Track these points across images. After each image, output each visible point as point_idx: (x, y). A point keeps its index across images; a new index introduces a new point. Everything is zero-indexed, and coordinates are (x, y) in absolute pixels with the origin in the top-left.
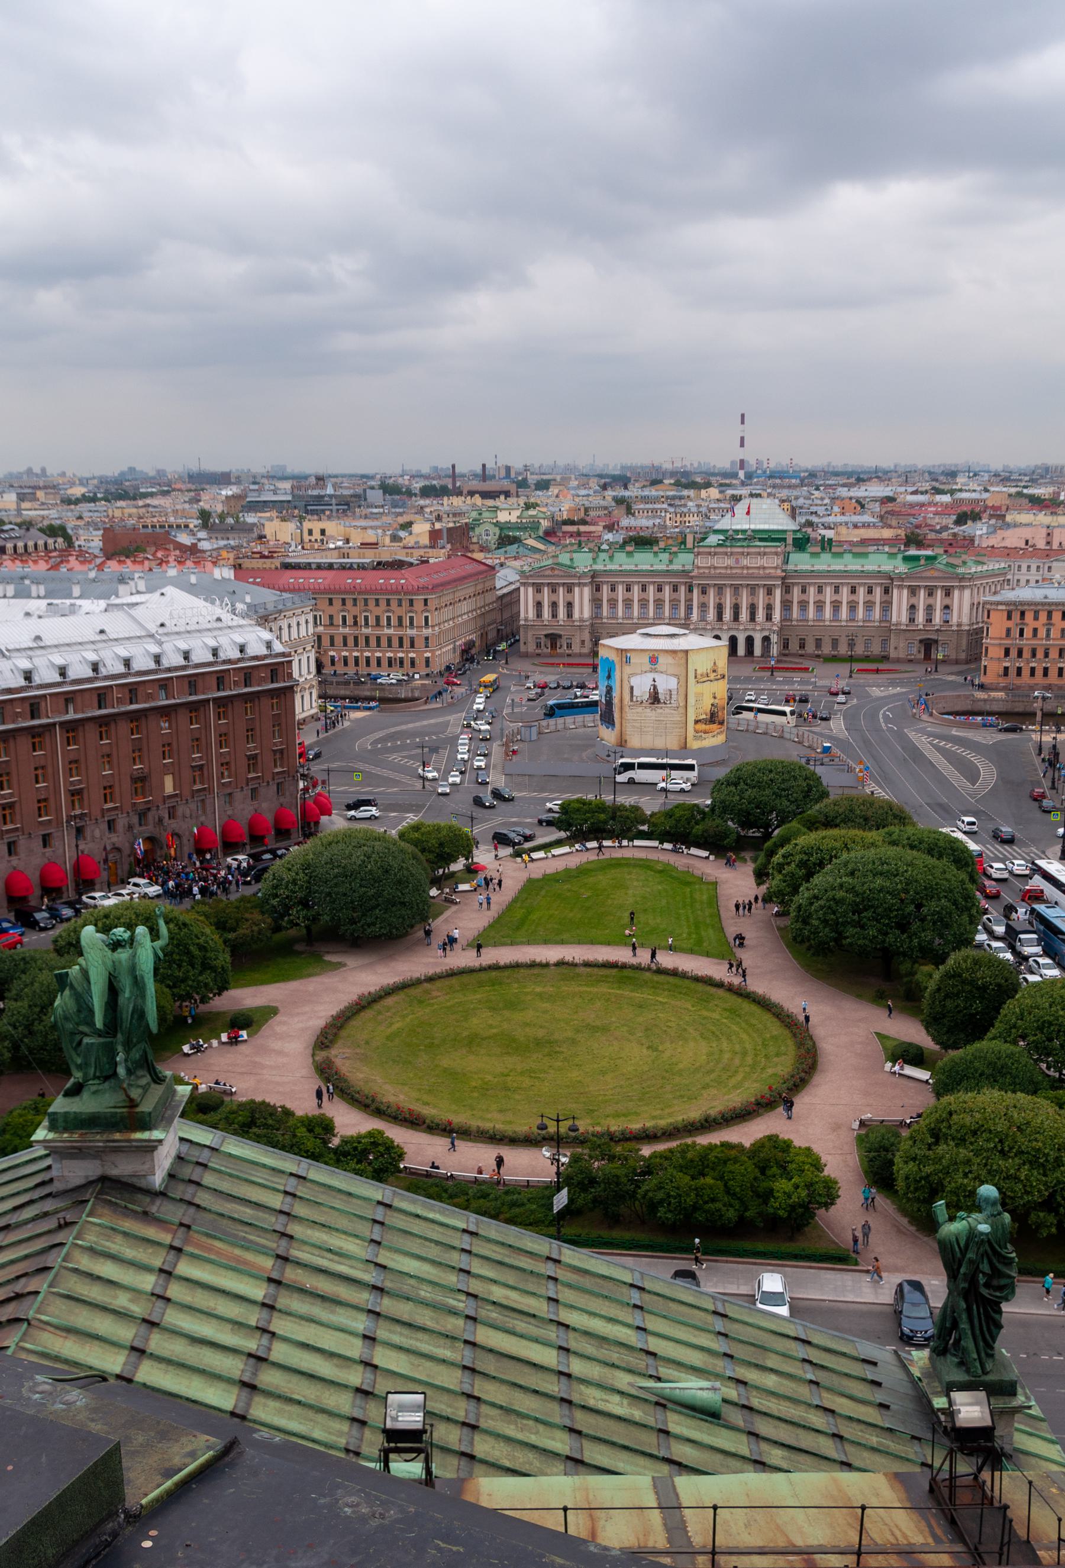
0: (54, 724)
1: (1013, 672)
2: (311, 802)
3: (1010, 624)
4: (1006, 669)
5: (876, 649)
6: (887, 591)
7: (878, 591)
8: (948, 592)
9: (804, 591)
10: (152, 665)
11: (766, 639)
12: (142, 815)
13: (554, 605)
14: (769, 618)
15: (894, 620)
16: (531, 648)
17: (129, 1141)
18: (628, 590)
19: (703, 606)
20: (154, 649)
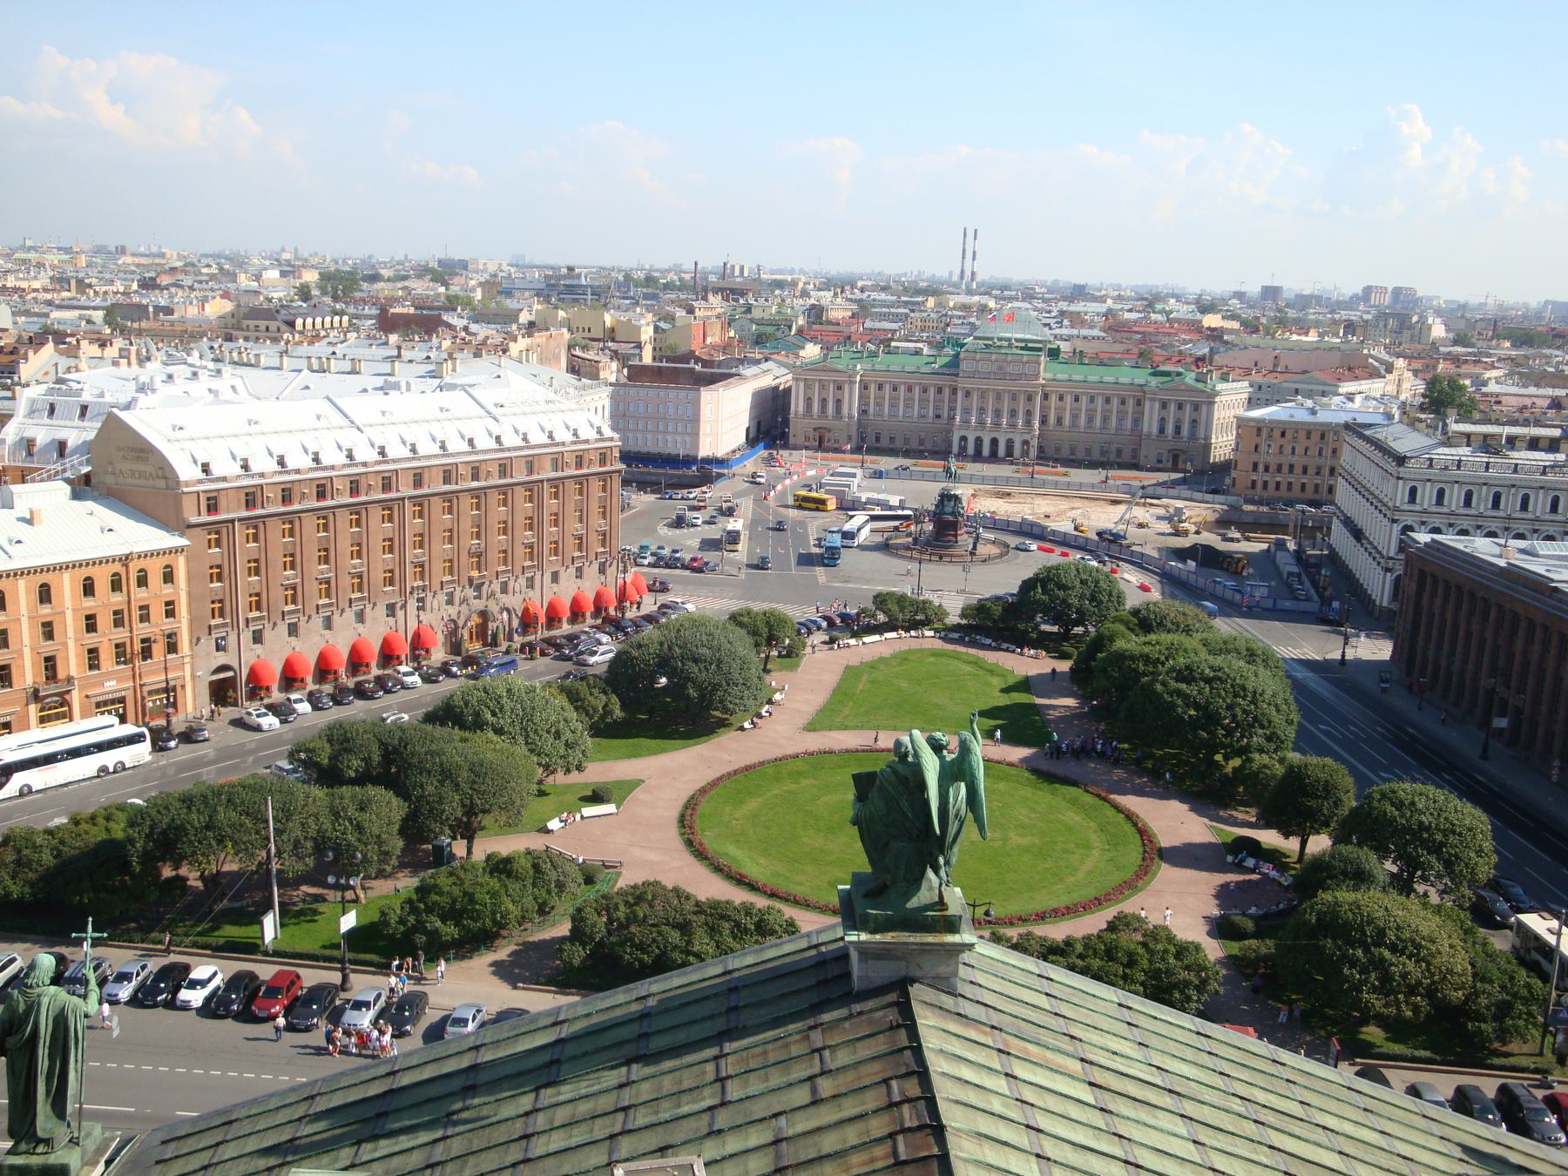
0: (403, 499)
1: (1259, 485)
2: (628, 580)
3: (1257, 440)
4: (1254, 482)
5: (1126, 457)
6: (1139, 403)
7: (1131, 403)
8: (1196, 407)
9: (1061, 398)
10: (494, 445)
11: (1026, 443)
12: (478, 588)
13: (824, 401)
14: (1028, 423)
15: (1145, 430)
16: (800, 440)
17: (943, 945)
18: (895, 389)
19: (967, 411)
20: (496, 431)
